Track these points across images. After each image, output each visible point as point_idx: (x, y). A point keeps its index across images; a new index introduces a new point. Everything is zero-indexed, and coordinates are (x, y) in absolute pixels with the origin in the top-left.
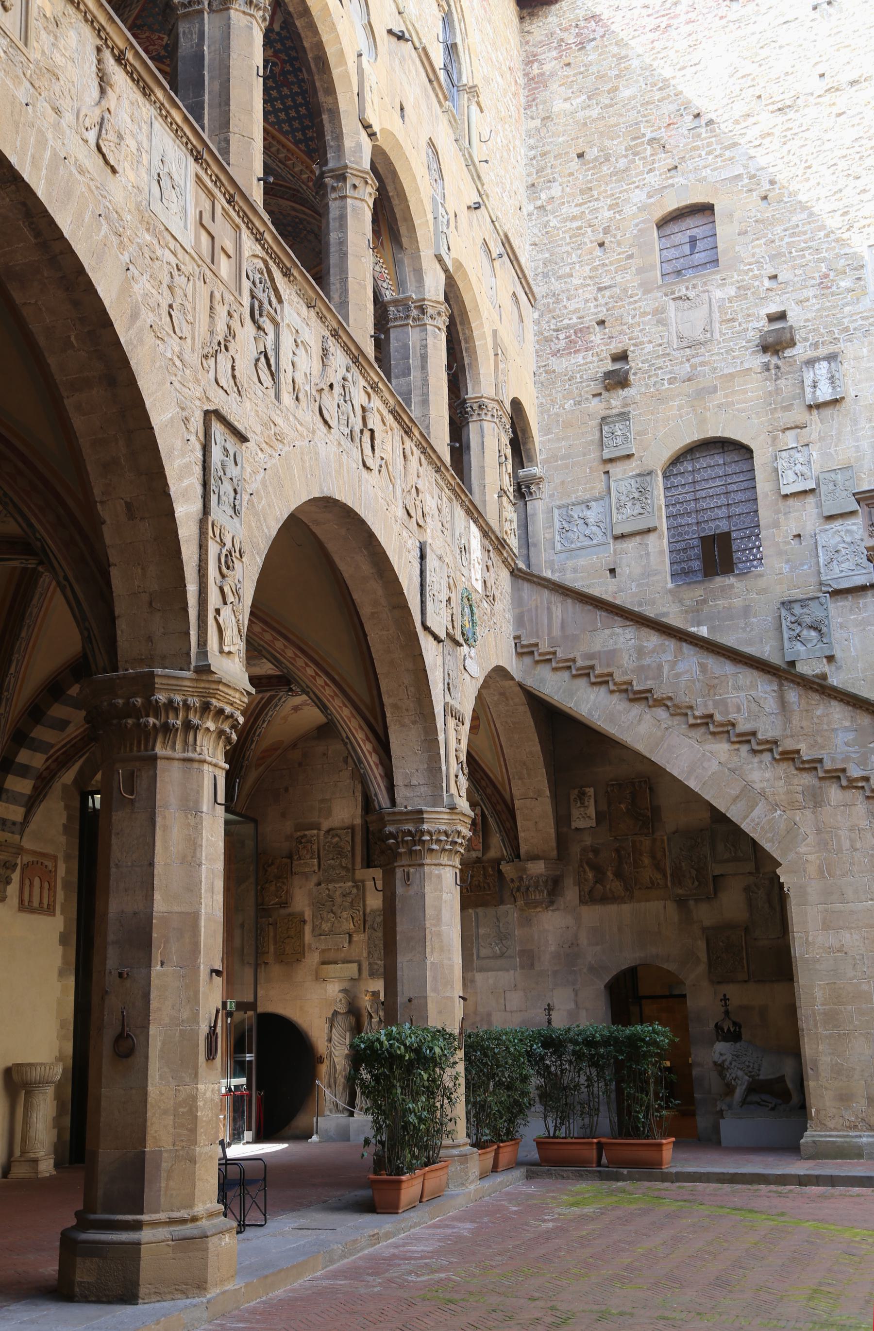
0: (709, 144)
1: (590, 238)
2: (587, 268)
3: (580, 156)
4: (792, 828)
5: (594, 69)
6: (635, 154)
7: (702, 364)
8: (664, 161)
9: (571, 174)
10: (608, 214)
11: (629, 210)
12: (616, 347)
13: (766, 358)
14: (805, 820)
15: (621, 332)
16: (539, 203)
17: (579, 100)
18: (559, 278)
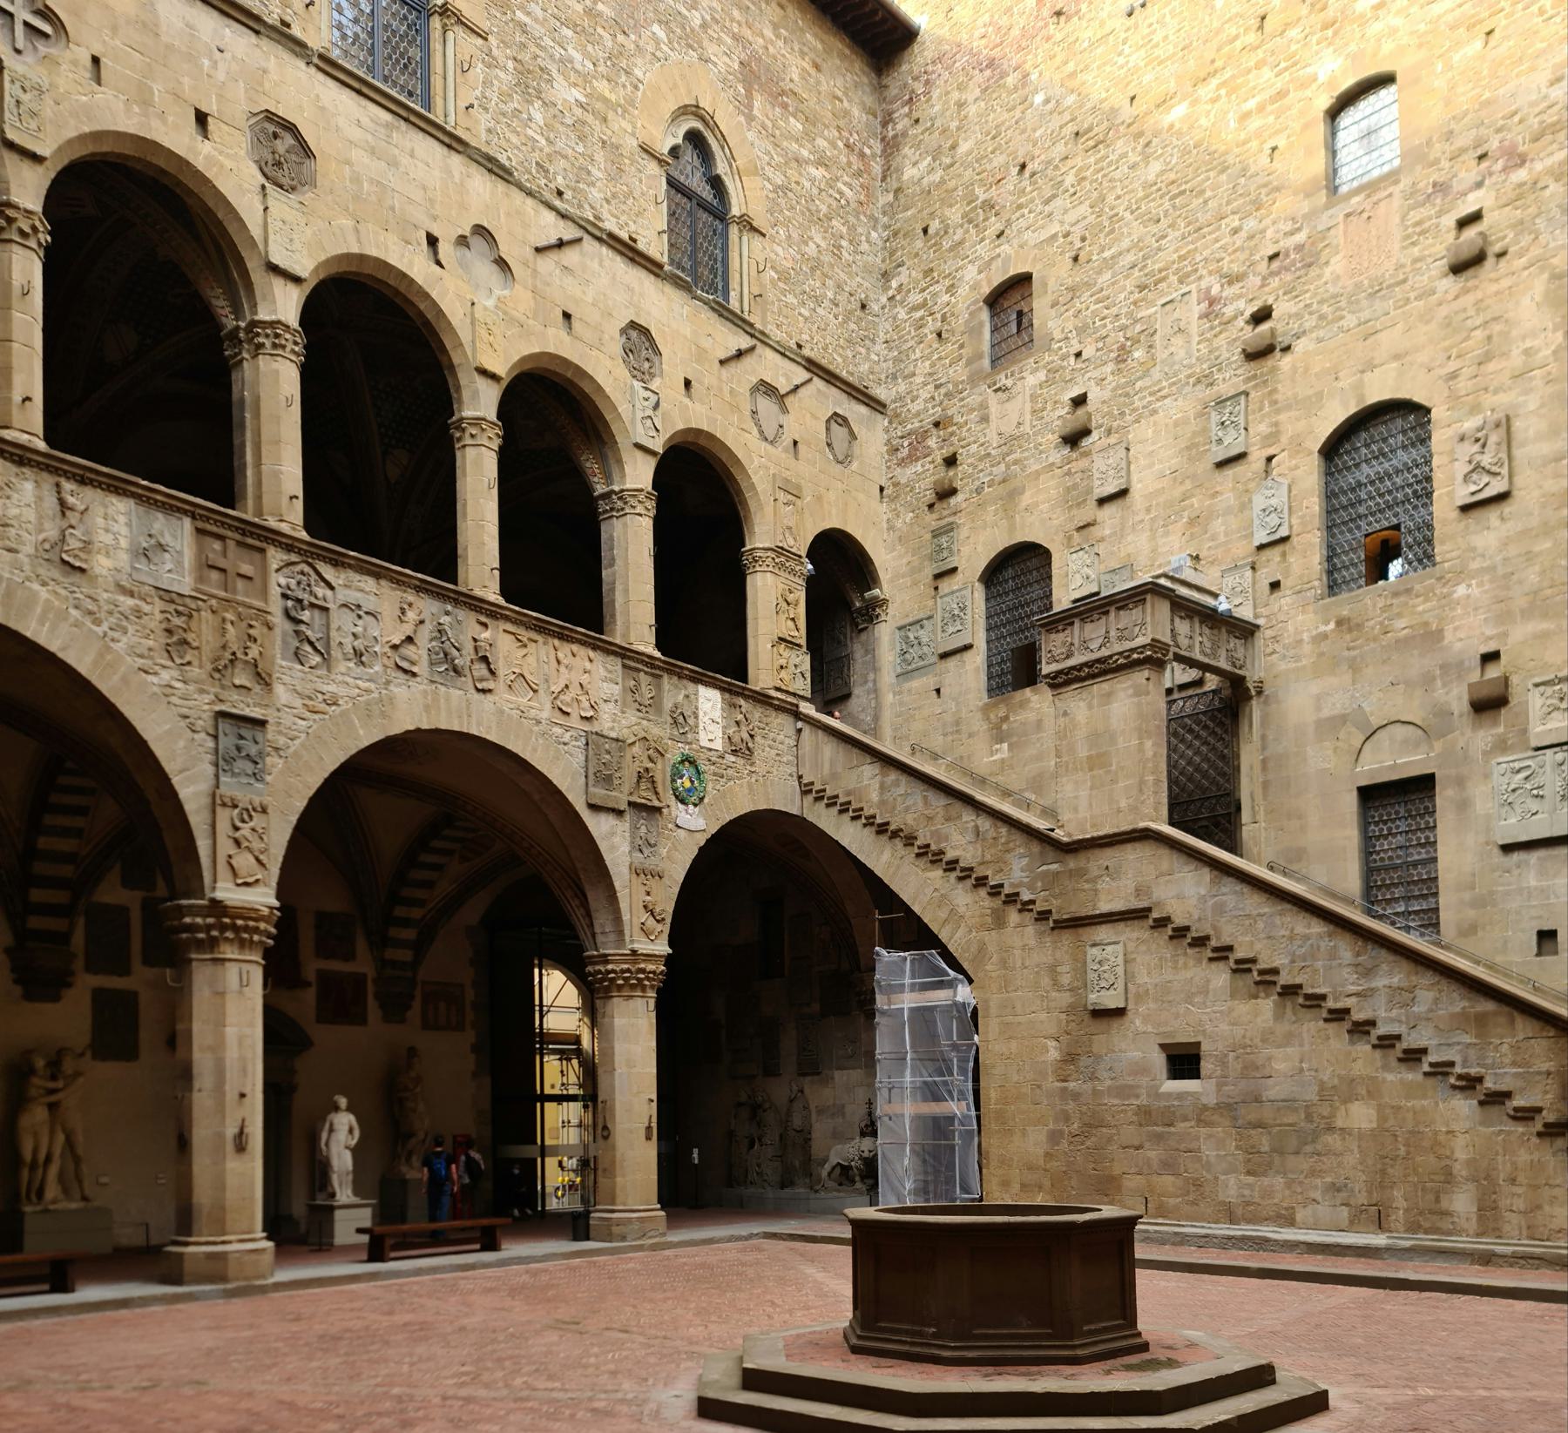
0: (1032, 201)
1: (932, 325)
2: (927, 363)
3: (925, 231)
4: (982, 948)
5: (938, 123)
6: (970, 222)
7: (1016, 462)
8: (995, 225)
9: (917, 255)
10: (946, 298)
11: (963, 291)
12: (946, 452)
13: (1066, 451)
14: (991, 938)
15: (952, 434)
16: (891, 293)
17: (925, 163)
18: (905, 378)
